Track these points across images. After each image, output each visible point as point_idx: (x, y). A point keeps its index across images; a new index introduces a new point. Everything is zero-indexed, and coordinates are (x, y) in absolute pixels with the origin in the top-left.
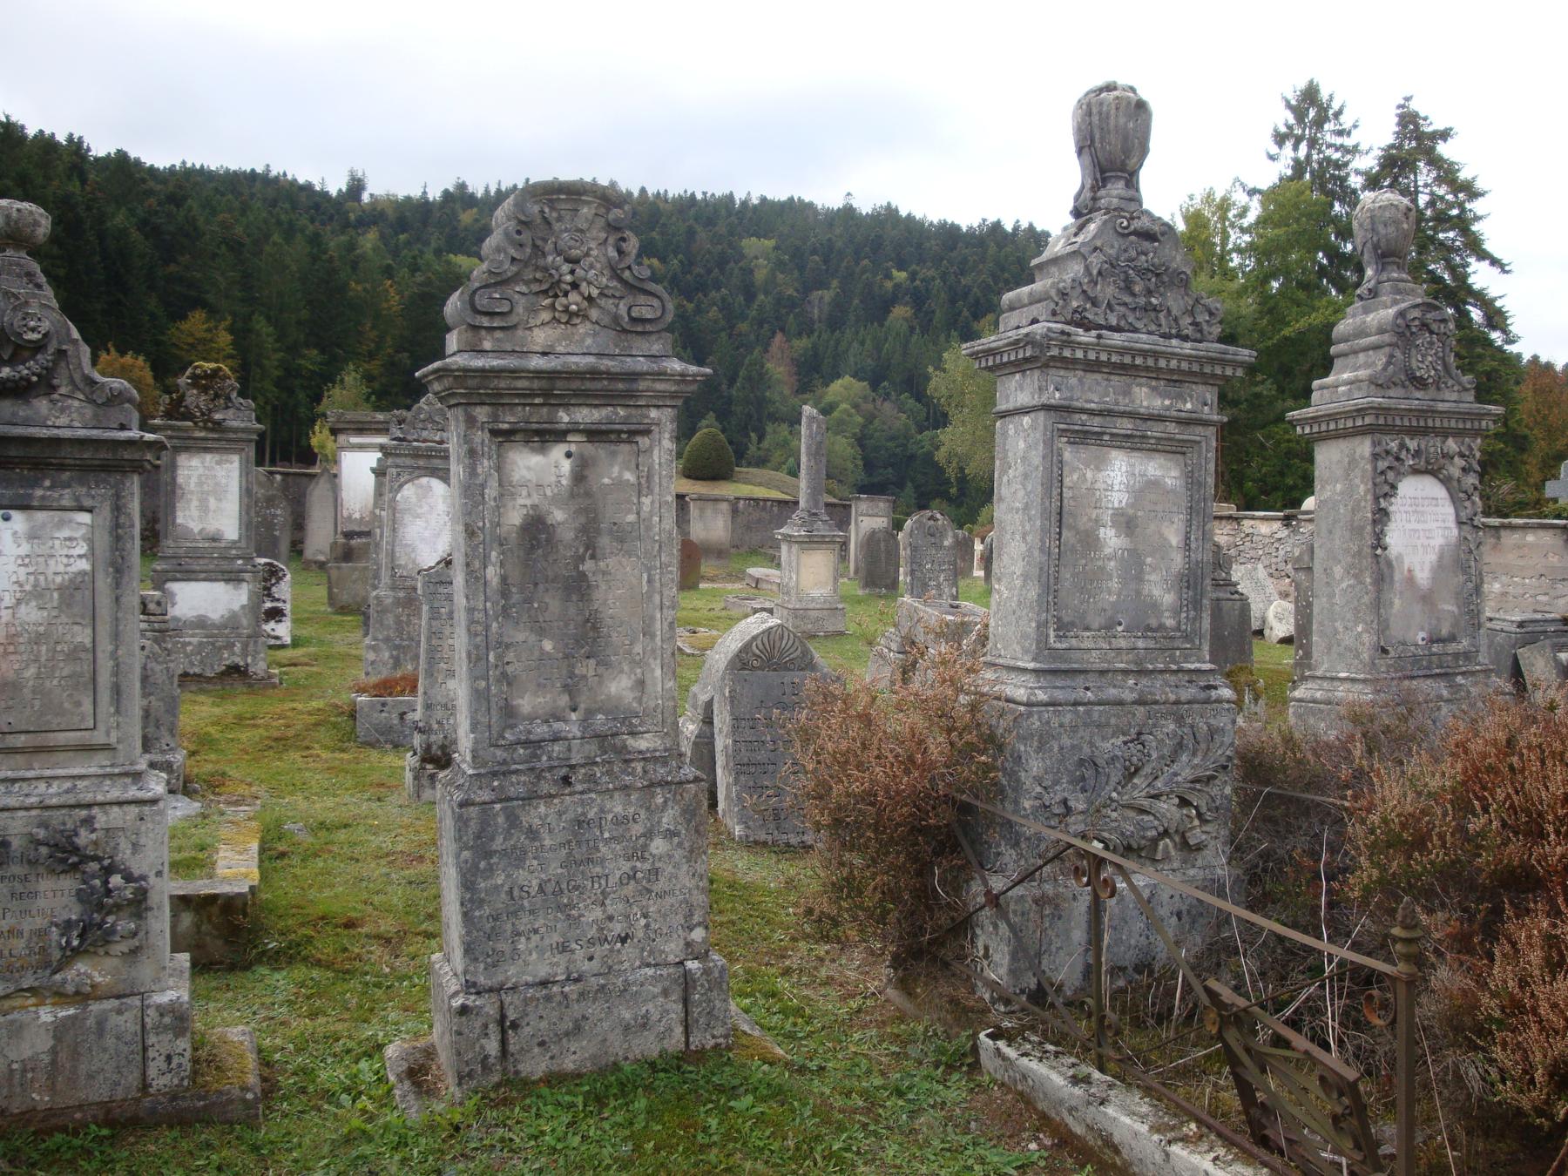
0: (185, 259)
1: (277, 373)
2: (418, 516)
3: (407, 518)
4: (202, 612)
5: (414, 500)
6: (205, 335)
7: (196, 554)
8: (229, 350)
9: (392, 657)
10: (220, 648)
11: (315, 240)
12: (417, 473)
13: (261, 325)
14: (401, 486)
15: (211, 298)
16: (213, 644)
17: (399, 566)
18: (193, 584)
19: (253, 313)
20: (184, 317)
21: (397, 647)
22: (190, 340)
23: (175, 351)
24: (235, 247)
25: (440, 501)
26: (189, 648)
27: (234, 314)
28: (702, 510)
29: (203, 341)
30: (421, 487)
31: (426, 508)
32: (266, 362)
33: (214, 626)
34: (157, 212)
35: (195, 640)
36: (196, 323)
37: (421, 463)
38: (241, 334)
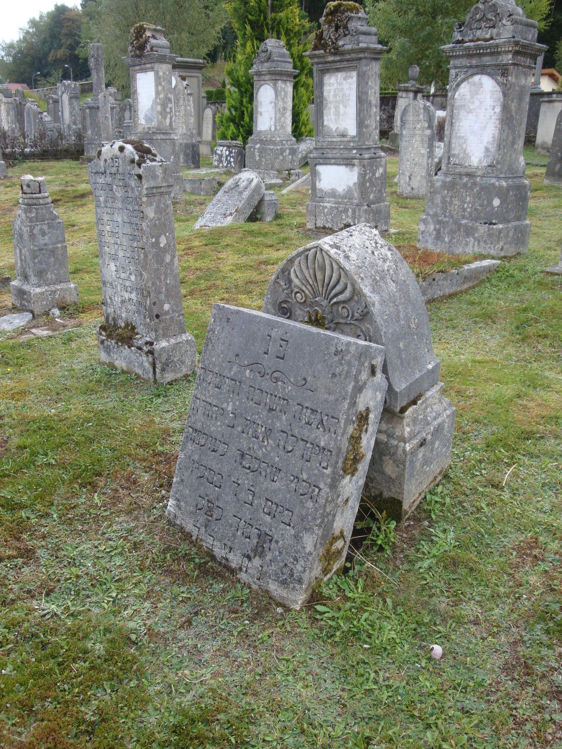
2: (470, 112)
3: (463, 113)
4: (333, 187)
5: (468, 97)
7: (332, 146)
9: (435, 229)
10: (341, 212)
12: (471, 71)
14: (458, 85)
16: (337, 208)
17: (454, 155)
18: (329, 167)
21: (439, 222)
25: (489, 96)
26: (326, 210)
30: (474, 84)
31: (477, 103)
33: (339, 195)
35: (328, 205)
37: (474, 62)
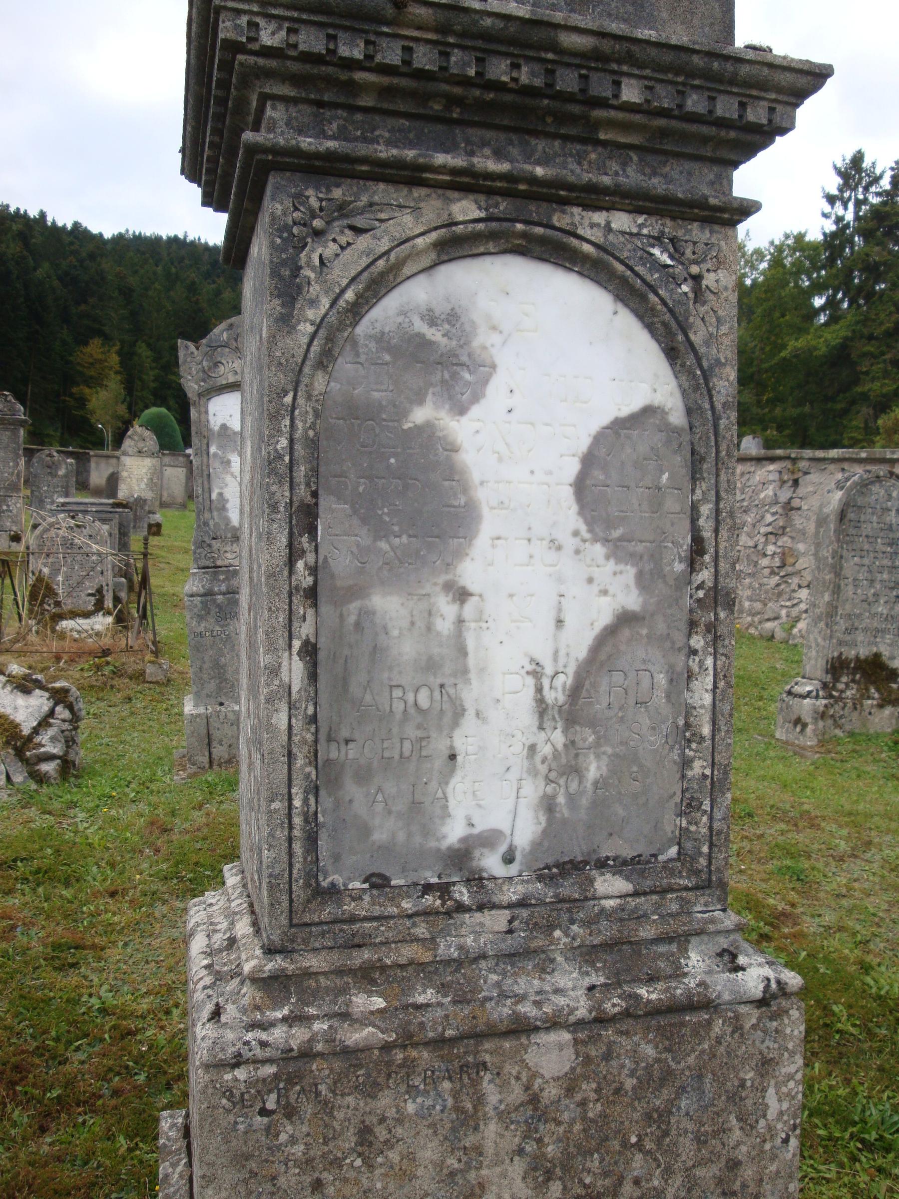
0: (91, 300)
1: (153, 385)
6: (100, 357)
8: (117, 367)
11: (192, 288)
13: (143, 350)
15: (106, 329)
19: (137, 341)
20: (86, 344)
22: (91, 360)
23: (80, 368)
24: (127, 293)
27: (122, 342)
28: (97, 463)
29: (101, 361)
32: (144, 377)
34: (75, 267)
36: (94, 348)
38: (127, 356)
